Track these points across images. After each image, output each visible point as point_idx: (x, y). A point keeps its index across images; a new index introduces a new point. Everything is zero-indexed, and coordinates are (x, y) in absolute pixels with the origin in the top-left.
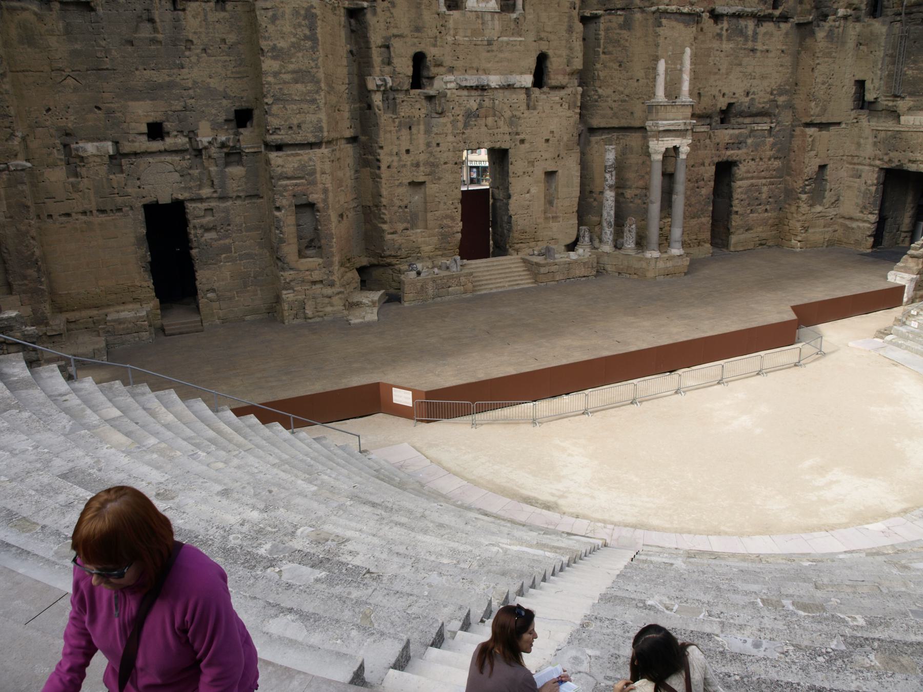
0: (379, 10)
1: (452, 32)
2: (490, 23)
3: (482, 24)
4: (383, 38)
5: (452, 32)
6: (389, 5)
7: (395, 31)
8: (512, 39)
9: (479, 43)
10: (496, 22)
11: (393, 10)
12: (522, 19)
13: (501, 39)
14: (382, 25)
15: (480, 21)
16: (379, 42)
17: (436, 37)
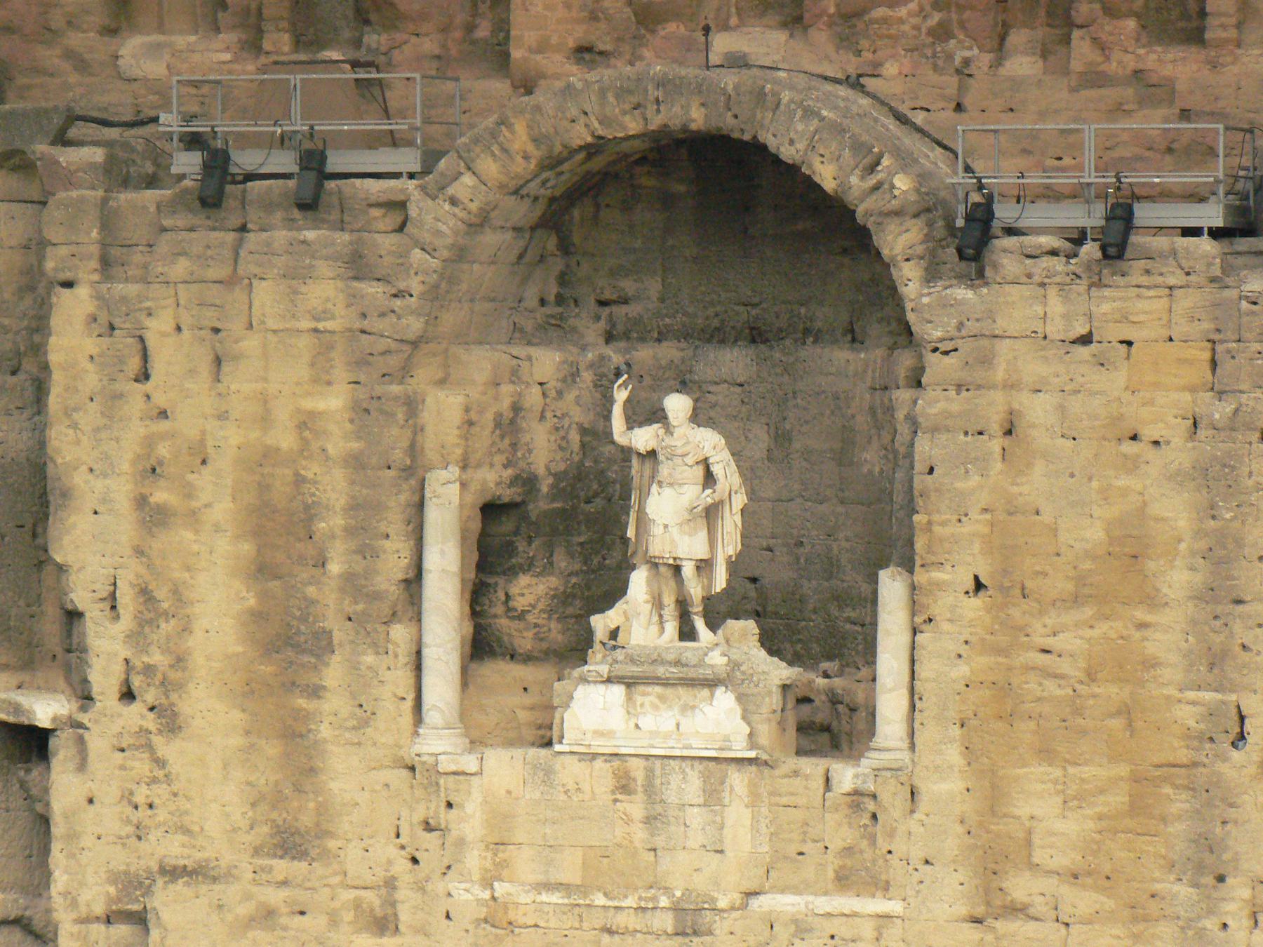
0: (97, 743)
1: (474, 860)
2: (696, 817)
3: (649, 820)
4: (114, 878)
5: (474, 860)
6: (150, 722)
7: (174, 849)
8: (823, 904)
9: (622, 920)
10: (738, 815)
11: (164, 747)
12: (892, 799)
13: (761, 904)
14: (109, 817)
15: (636, 808)
16: (96, 896)
17: (390, 884)
